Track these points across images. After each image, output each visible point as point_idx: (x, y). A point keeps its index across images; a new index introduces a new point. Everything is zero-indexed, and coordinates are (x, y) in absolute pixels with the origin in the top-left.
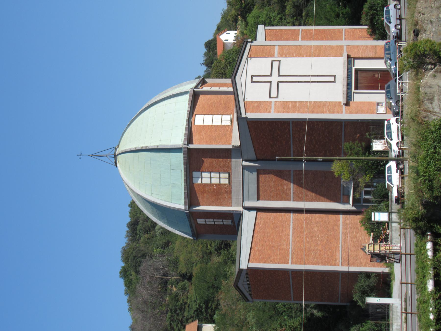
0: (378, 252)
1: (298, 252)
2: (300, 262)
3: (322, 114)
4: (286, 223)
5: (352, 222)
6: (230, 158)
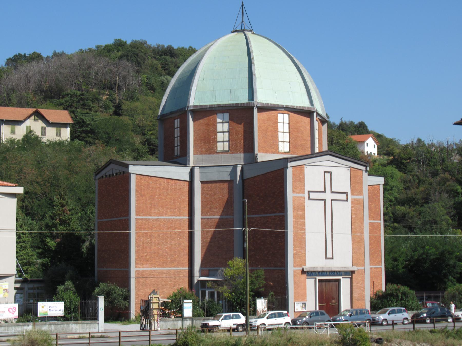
0: (151, 308)
1: (149, 225)
2: (138, 228)
4: (179, 212)
5: (181, 280)
6: (244, 153)
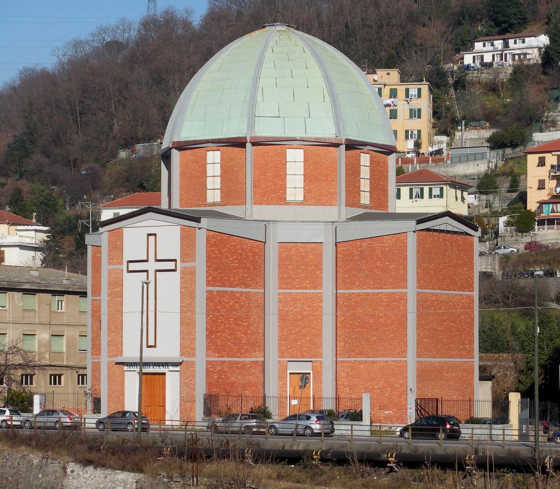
3: (107, 332)
